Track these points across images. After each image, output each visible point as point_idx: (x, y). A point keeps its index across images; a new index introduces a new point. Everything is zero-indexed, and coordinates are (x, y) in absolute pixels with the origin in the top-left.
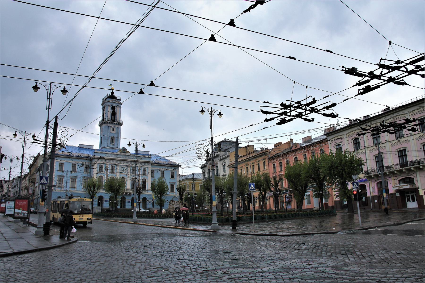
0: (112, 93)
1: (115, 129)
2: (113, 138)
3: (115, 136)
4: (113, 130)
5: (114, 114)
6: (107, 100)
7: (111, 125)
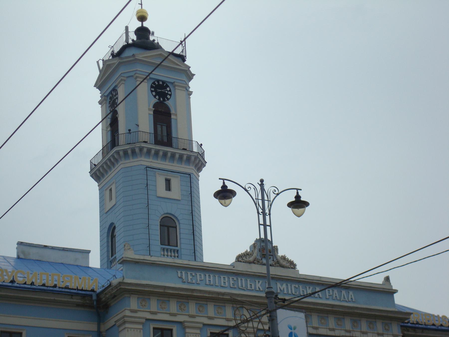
0: (143, 32)
1: (175, 183)
2: (168, 226)
3: (180, 213)
5: (163, 116)
6: (128, 53)
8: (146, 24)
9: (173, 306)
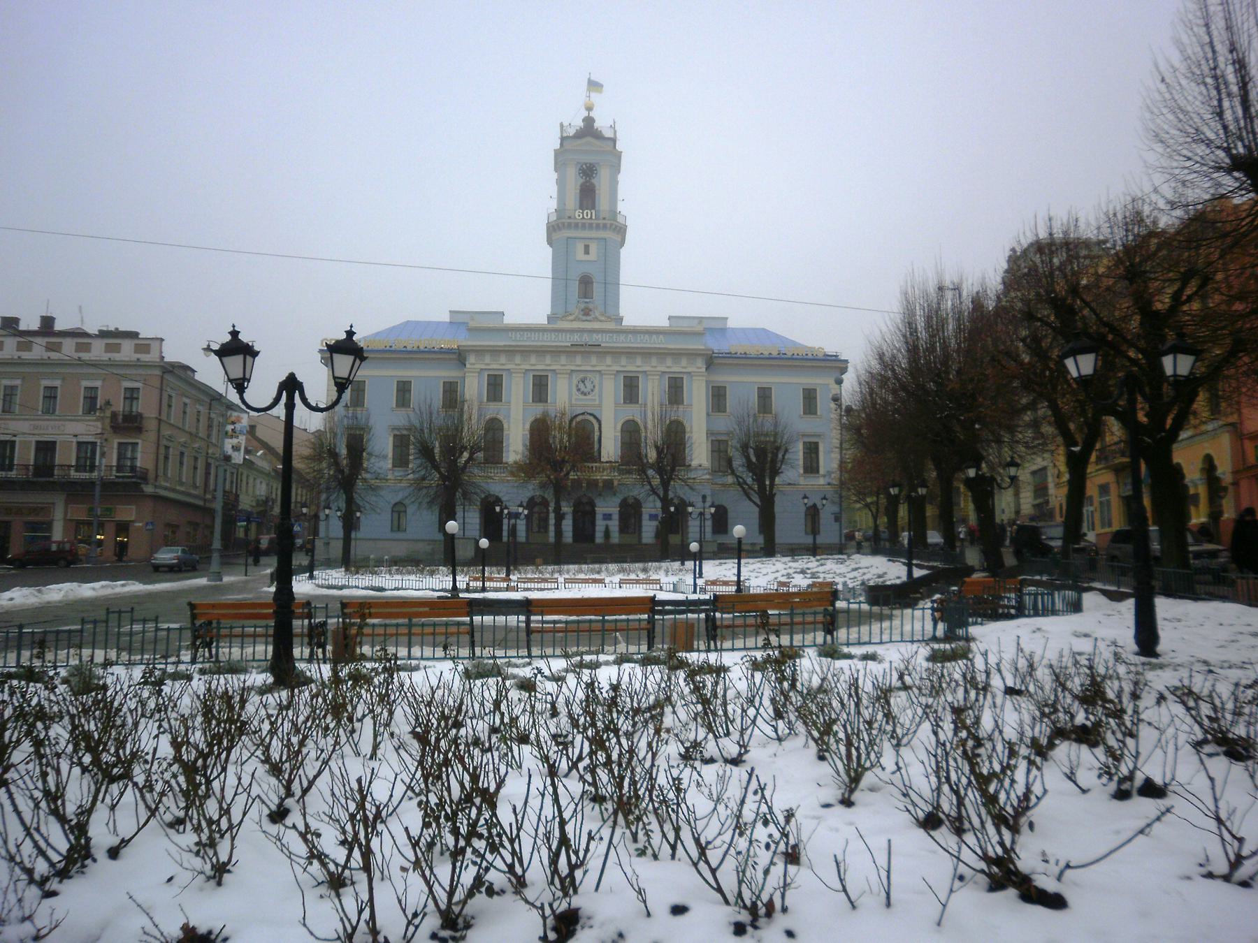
0: (589, 121)
1: (593, 248)
2: (586, 283)
4: (587, 252)
8: (592, 114)
9: (503, 359)
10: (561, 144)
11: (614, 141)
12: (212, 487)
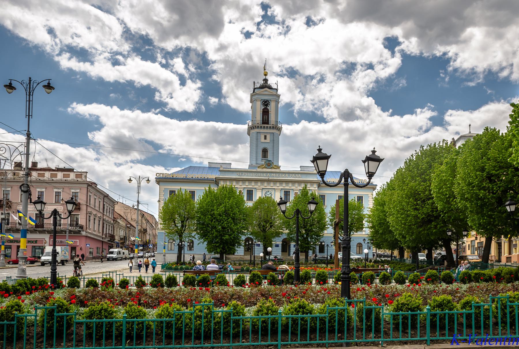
0: (266, 80)
1: (268, 137)
2: (265, 151)
4: (265, 138)
5: (266, 112)
7: (262, 131)
10: (254, 91)
11: (277, 90)
12: (105, 233)
